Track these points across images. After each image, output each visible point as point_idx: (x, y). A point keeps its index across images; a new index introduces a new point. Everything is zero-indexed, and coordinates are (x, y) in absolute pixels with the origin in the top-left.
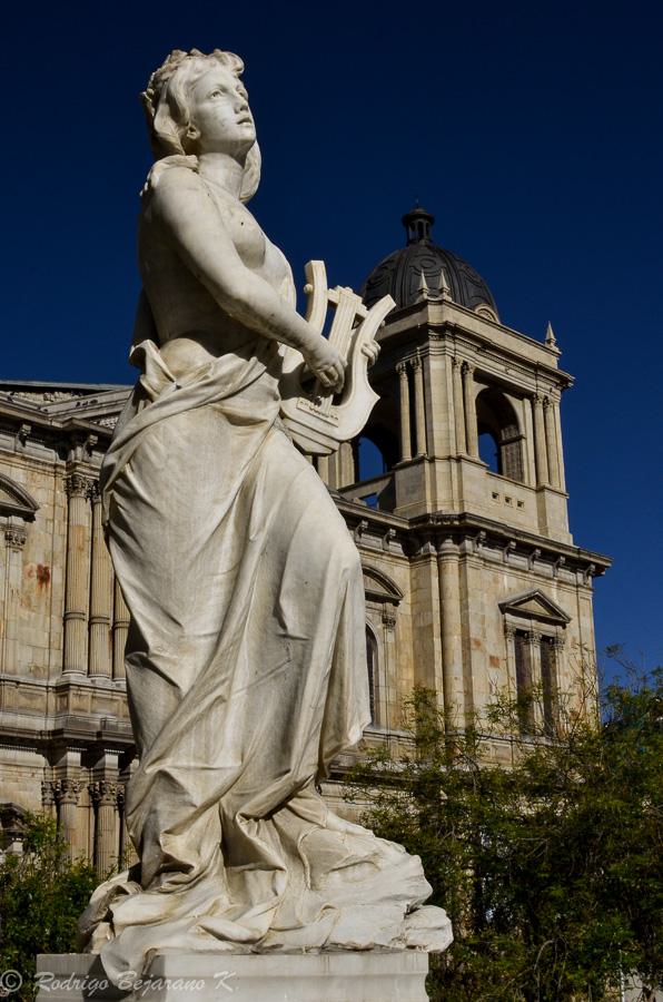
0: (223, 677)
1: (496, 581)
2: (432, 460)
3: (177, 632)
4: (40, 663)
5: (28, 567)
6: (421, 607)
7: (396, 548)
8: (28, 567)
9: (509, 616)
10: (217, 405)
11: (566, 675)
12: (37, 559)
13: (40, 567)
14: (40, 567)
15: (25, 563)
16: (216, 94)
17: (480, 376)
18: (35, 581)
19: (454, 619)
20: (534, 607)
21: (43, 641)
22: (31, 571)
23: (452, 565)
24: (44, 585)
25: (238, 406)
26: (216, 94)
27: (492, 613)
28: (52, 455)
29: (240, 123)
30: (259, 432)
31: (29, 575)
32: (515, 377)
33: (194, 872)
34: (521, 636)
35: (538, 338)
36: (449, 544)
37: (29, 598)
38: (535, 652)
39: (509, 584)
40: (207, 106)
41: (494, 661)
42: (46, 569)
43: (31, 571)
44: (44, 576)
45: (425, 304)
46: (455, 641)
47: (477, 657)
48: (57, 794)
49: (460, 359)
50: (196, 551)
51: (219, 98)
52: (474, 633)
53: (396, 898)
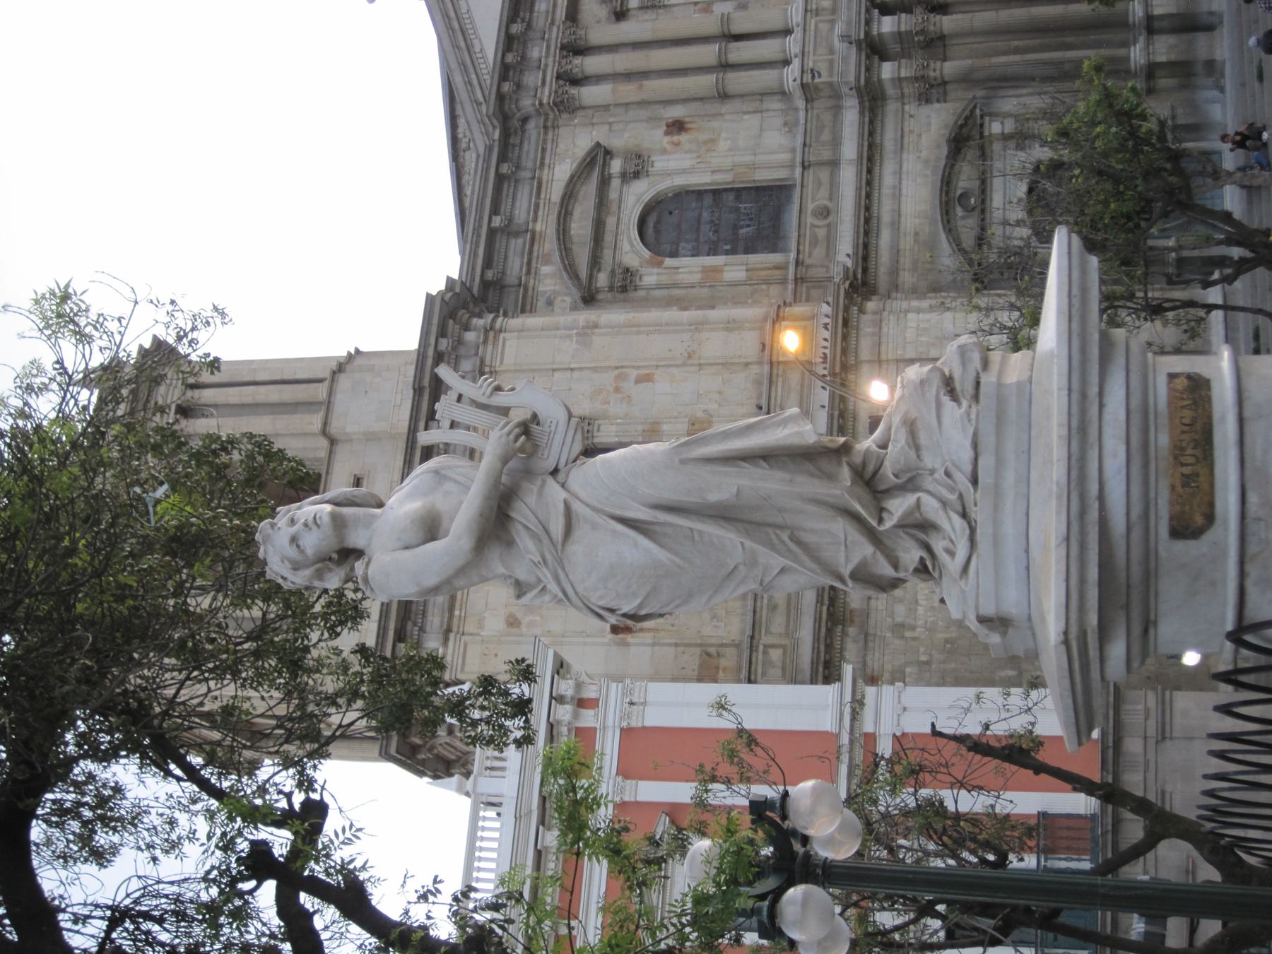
0: (773, 537)
3: (741, 567)
4: (779, 121)
5: (668, 147)
8: (668, 147)
10: (559, 547)
12: (655, 137)
13: (667, 133)
14: (667, 133)
16: (298, 546)
18: (683, 138)
21: (752, 121)
22: (673, 143)
24: (688, 126)
25: (557, 528)
26: (298, 546)
29: (318, 526)
30: (577, 506)
31: (678, 144)
33: (925, 555)
37: (705, 142)
40: (310, 552)
42: (668, 126)
43: (673, 143)
44: (678, 126)
48: (931, 90)
50: (677, 560)
51: (301, 543)
53: (939, 406)
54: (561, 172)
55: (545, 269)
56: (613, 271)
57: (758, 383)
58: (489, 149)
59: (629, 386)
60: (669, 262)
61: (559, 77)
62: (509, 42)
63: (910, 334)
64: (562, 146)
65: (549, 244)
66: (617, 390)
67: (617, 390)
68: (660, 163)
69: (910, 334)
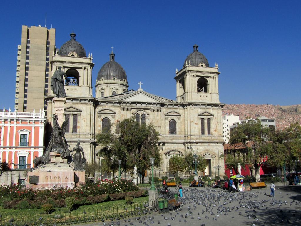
1: (197, 111)
2: (187, 92)
6: (185, 116)
7: (181, 107)
9: (199, 116)
11: (214, 124)
15: (115, 120)
17: (197, 76)
19: (189, 118)
20: (206, 114)
23: (188, 109)
27: (196, 116)
28: (118, 105)
32: (206, 75)
34: (203, 119)
35: (214, 67)
36: (188, 106)
38: (206, 121)
39: (200, 110)
41: (196, 124)
45: (186, 67)
46: (189, 121)
47: (192, 123)
49: (192, 75)
52: (192, 120)
54: (113, 109)
55: (101, 107)
56: (100, 115)
57: (84, 133)
58: (116, 100)
59: (84, 119)
60: (101, 121)
61: (124, 108)
62: (128, 102)
63: (87, 148)
64: (117, 108)
65: (105, 108)
66: (83, 118)
67: (83, 118)
68: (114, 119)
69: (87, 148)
